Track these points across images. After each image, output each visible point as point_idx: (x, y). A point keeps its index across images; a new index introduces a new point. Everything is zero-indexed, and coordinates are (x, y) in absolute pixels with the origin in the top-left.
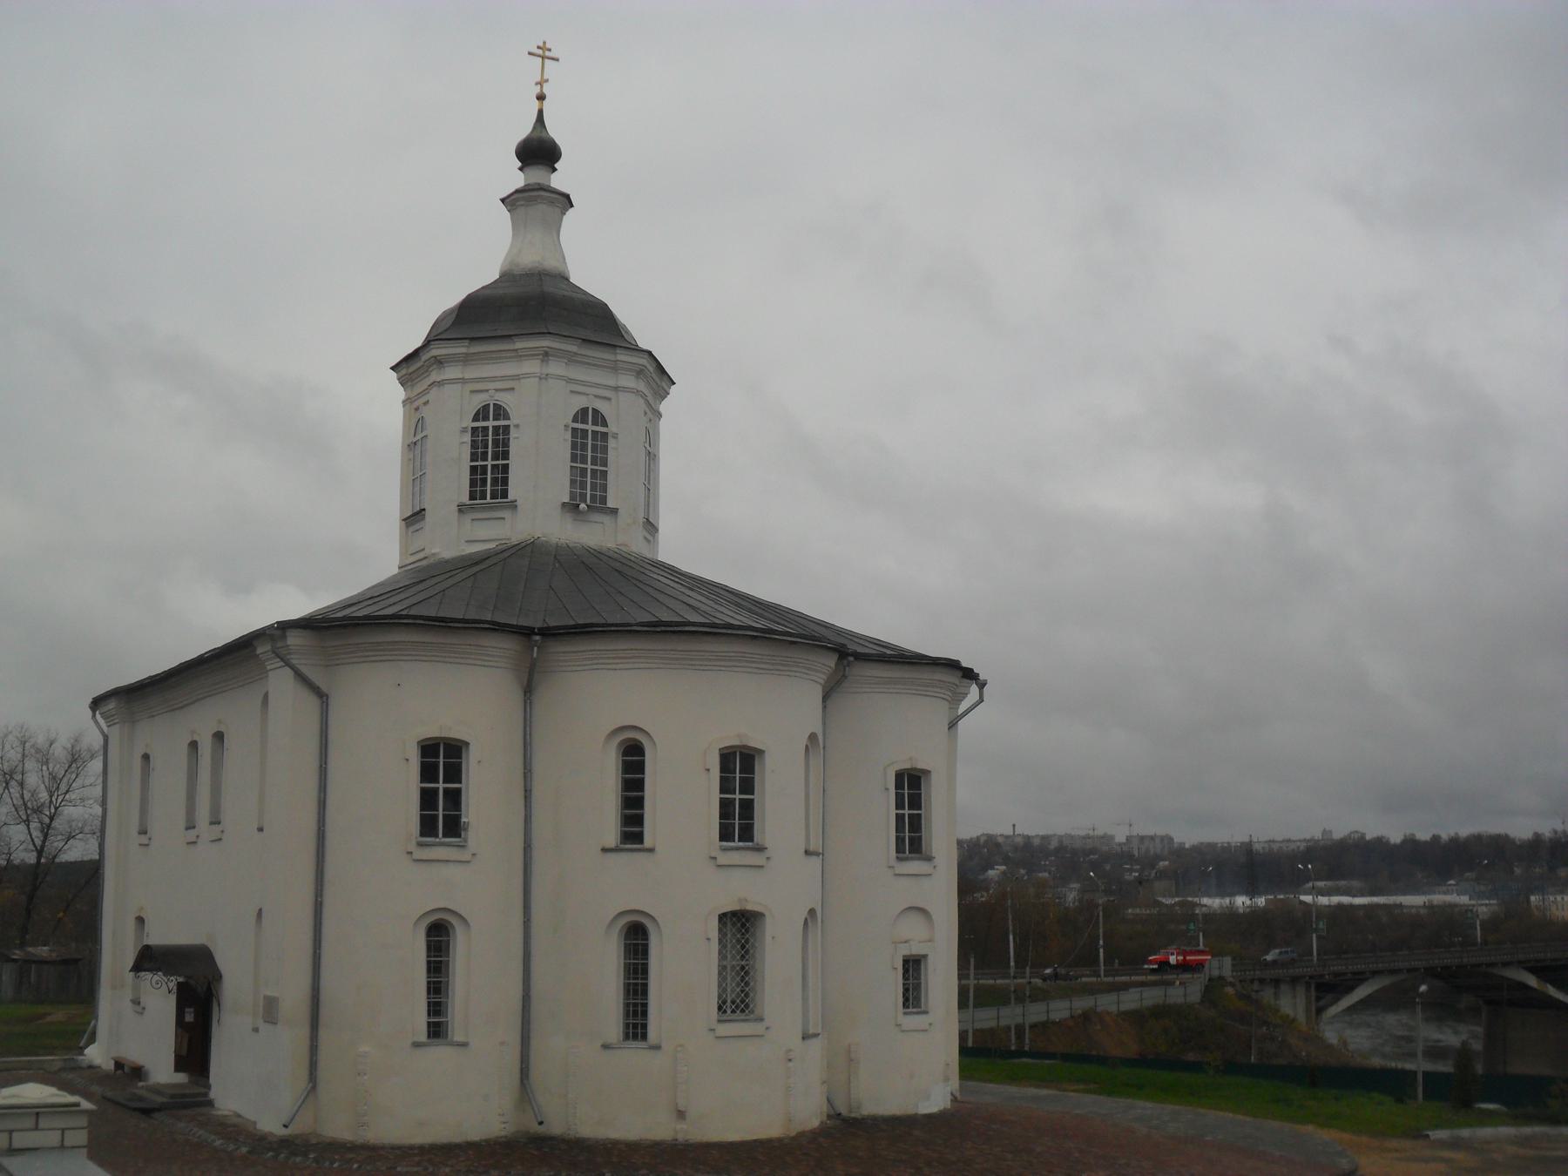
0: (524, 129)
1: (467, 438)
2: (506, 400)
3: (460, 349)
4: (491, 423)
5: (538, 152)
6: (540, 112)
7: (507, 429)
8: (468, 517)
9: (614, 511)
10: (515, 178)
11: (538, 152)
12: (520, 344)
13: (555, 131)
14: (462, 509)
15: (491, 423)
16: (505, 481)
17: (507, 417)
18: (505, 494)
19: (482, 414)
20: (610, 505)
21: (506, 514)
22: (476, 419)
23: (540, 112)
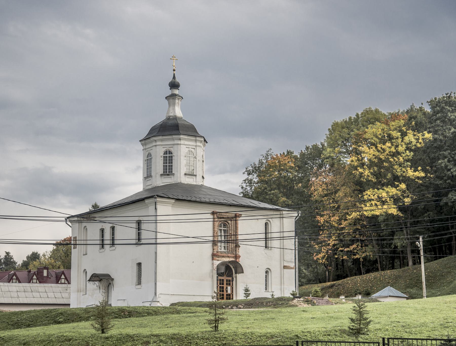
0: (171, 79)
1: (162, 158)
2: (172, 149)
3: (161, 138)
4: (168, 155)
5: (174, 85)
6: (174, 74)
7: (172, 157)
8: (163, 177)
9: (196, 176)
10: (169, 92)
11: (174, 85)
12: (174, 137)
13: (177, 80)
14: (161, 175)
15: (168, 155)
16: (172, 169)
17: (172, 154)
18: (172, 172)
19: (166, 153)
20: (195, 174)
21: (172, 176)
22: (164, 154)
23: (174, 74)
